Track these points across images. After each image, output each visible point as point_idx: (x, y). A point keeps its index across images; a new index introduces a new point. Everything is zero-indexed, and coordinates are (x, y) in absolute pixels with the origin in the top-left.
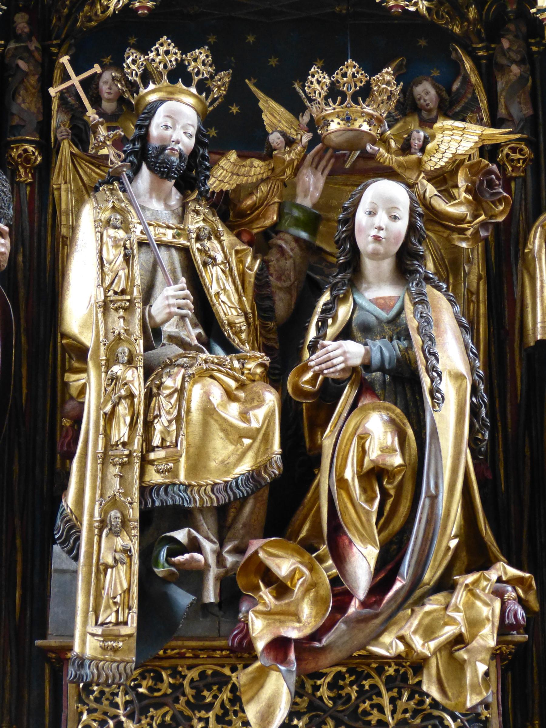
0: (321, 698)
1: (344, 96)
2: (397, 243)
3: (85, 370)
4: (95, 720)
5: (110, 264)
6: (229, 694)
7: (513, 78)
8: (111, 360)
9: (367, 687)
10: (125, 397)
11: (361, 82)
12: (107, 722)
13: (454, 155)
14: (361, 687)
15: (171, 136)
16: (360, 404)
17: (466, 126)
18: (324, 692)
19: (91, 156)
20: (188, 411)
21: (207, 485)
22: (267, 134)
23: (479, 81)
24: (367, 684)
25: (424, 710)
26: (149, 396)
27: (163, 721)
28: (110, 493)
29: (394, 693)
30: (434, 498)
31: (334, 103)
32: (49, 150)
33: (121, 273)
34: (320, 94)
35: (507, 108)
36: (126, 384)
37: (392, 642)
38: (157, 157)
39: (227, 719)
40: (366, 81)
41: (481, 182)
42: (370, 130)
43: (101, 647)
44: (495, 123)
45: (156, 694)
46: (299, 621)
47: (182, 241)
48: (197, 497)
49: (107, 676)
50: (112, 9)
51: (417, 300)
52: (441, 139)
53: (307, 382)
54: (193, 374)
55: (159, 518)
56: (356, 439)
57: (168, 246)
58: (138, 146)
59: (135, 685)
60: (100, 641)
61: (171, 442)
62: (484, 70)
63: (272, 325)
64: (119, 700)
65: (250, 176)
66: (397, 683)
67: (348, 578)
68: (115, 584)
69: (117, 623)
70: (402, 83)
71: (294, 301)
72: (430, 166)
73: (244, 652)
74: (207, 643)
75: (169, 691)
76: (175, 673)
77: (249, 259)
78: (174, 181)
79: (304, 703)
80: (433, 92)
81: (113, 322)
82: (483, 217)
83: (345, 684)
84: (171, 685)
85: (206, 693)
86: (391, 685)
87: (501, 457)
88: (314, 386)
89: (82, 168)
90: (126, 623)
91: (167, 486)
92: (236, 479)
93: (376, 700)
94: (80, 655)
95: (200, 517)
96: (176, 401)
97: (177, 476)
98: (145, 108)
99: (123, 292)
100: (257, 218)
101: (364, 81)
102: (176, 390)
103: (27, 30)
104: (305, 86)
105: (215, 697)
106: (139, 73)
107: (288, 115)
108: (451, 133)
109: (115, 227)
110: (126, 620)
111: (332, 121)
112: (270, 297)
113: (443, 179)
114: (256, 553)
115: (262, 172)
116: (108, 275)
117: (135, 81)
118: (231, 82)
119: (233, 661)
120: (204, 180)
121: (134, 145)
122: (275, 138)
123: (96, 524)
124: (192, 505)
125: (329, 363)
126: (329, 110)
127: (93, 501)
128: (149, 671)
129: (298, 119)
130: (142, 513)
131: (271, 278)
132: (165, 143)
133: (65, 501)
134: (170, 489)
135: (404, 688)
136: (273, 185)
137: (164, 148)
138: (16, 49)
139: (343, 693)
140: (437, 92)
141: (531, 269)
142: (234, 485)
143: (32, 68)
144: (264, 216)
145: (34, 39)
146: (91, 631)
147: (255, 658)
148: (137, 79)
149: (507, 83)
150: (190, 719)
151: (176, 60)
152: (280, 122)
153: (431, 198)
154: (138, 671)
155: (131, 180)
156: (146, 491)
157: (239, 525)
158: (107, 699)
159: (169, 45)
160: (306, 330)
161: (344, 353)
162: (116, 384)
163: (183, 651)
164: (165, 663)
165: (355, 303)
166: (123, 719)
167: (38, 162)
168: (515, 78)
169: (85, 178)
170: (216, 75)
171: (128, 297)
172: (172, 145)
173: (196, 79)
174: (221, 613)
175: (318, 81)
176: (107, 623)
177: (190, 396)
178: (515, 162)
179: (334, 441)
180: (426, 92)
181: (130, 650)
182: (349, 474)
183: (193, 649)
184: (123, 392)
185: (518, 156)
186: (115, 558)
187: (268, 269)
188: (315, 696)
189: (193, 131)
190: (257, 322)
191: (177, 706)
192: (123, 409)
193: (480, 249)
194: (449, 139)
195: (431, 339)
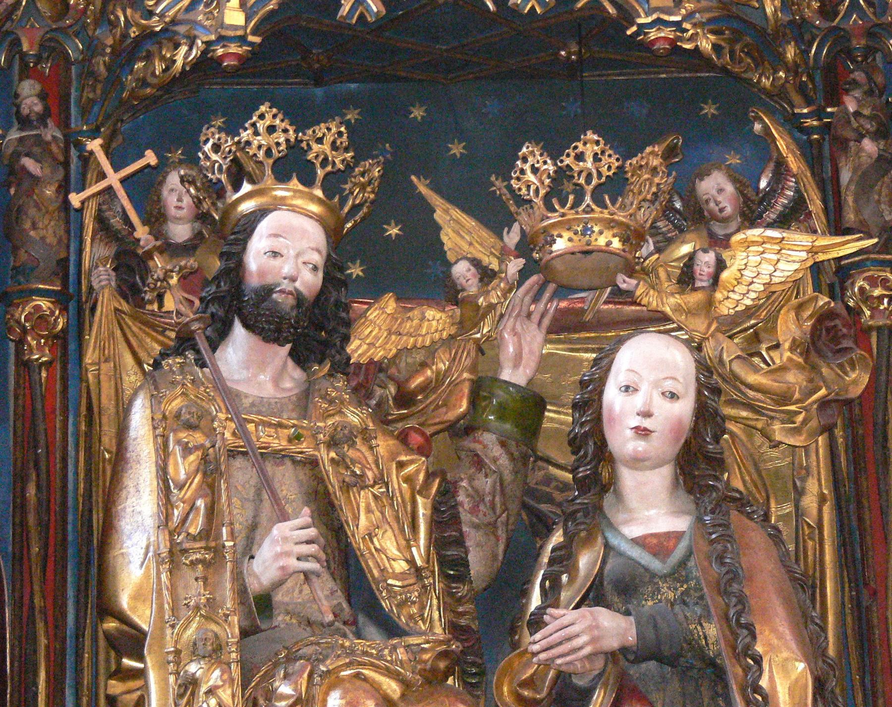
2: (677, 439)
3: (140, 674)
5: (181, 489)
7: (864, 159)
13: (768, 285)
17: (785, 235)
22: (449, 265)
31: (563, 205)
32: (75, 301)
33: (200, 503)
34: (537, 191)
35: (858, 211)
38: (257, 305)
42: (624, 250)
44: (837, 227)
47: (305, 447)
50: (179, 62)
51: (714, 536)
52: (745, 261)
57: (280, 456)
63: (462, 590)
65: (420, 335)
70: (674, 173)
78: (288, 346)
80: (730, 188)
81: (186, 587)
82: (823, 392)
89: (134, 335)
98: (236, 225)
103: (39, 108)
104: (512, 178)
106: (224, 167)
107: (485, 233)
108: (761, 249)
109: (191, 427)
111: (560, 236)
112: (460, 542)
113: (752, 329)
115: (440, 329)
116: (177, 507)
117: (219, 181)
118: (381, 177)
121: (218, 286)
122: (461, 270)
126: (554, 218)
129: (502, 239)
131: (461, 509)
136: (460, 351)
138: (21, 139)
143: (47, 171)
145: (50, 123)
148: (223, 178)
149: (855, 170)
151: (287, 141)
152: (471, 244)
153: (731, 362)
155: (214, 347)
159: (274, 116)
160: (525, 594)
161: (591, 628)
167: (60, 327)
168: (869, 160)
170: (356, 164)
171: (213, 544)
172: (286, 285)
175: (533, 169)
189: (317, 259)
193: (821, 451)
194: (758, 259)
195: (742, 600)
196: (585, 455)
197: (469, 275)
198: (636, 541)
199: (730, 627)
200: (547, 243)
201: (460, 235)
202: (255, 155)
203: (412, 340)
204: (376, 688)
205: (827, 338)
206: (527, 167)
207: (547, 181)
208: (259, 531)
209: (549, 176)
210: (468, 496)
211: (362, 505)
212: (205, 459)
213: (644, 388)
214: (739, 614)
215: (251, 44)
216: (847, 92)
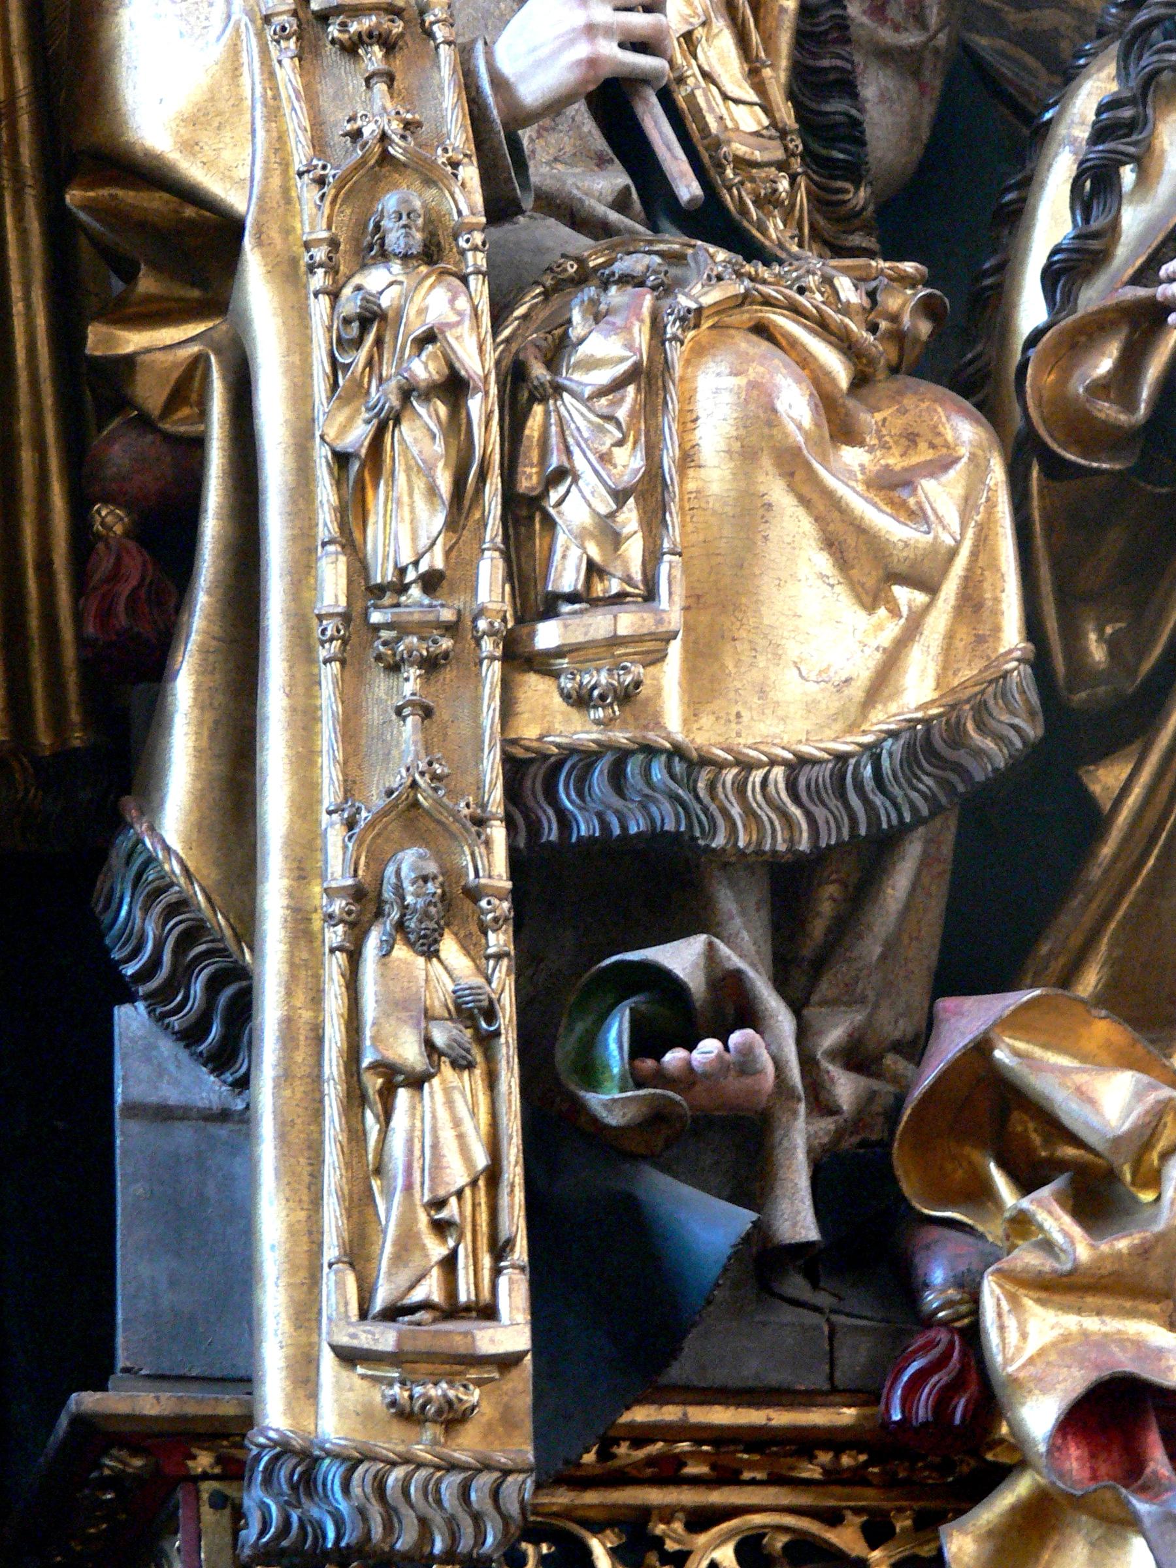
10: (429, 393)
20: (688, 459)
21: (773, 763)
48: (736, 811)
49: (424, 1523)
53: (1100, 388)
54: (699, 310)
63: (860, 196)
69: (452, 1310)
71: (929, 109)
74: (781, 1418)
88: (1129, 405)
90: (488, 1312)
91: (622, 756)
92: (873, 751)
94: (297, 1443)
96: (633, 414)
102: (633, 375)
112: (847, 86)
114: (982, 1048)
119: (870, 1497)
123: (338, 906)
124: (719, 841)
133: (152, 829)
134: (632, 767)
146: (344, 1340)
147: (993, 1478)
162: (379, 342)
163: (685, 1446)
177: (688, 399)
181: (507, 1419)
183: (723, 1438)
186: (429, 1045)
192: (420, 437)
204: (805, 361)
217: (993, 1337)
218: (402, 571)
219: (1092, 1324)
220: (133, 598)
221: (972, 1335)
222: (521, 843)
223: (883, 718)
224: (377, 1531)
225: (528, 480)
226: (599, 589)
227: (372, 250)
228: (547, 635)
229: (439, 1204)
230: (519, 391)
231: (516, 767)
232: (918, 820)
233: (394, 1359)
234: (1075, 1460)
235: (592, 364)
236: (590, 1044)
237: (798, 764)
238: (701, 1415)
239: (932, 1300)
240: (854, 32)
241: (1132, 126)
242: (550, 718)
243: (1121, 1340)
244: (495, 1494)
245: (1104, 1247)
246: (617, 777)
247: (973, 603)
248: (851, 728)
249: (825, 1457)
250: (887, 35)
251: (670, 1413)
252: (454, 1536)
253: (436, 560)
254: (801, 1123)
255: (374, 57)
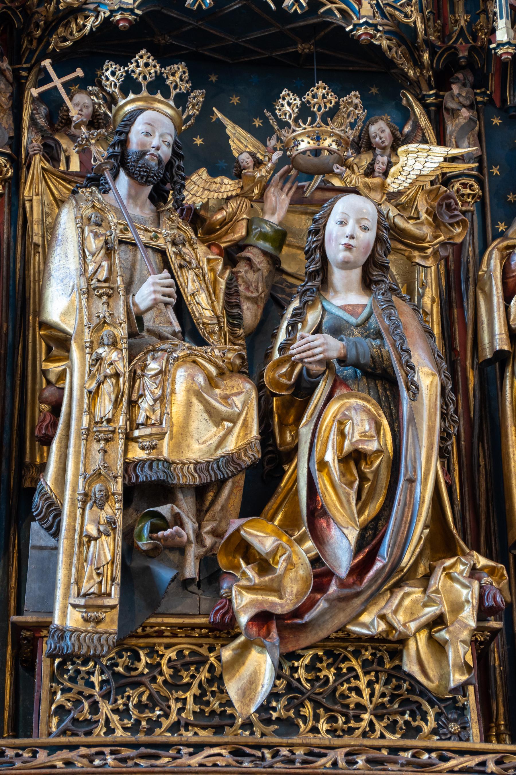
0: (299, 680)
1: (313, 115)
2: (366, 253)
4: (69, 700)
6: (207, 675)
8: (95, 343)
9: (344, 670)
10: (111, 376)
11: (331, 103)
12: (81, 702)
14: (339, 669)
15: (151, 143)
16: (336, 396)
18: (302, 674)
19: (62, 172)
20: (173, 392)
21: (190, 463)
23: (429, 125)
24: (344, 666)
25: (402, 695)
26: (133, 377)
27: (140, 701)
28: (93, 467)
29: (372, 676)
30: (411, 481)
31: (305, 123)
34: (290, 116)
36: (111, 364)
37: (374, 620)
39: (204, 699)
40: (336, 102)
41: (440, 205)
43: (83, 617)
45: (133, 673)
46: (281, 598)
47: (161, 243)
48: (180, 475)
49: (88, 647)
50: (88, 28)
54: (178, 357)
55: (146, 492)
56: (336, 423)
58: (117, 149)
59: (111, 664)
60: (82, 612)
61: (156, 420)
62: (432, 116)
63: (240, 332)
64: (96, 679)
66: (375, 666)
67: (328, 558)
68: (99, 555)
69: (100, 595)
71: (260, 311)
72: (393, 188)
73: (224, 629)
74: (187, 621)
75: (146, 671)
76: (152, 652)
77: (220, 267)
79: (282, 684)
80: (388, 131)
82: (442, 238)
83: (323, 666)
84: (147, 665)
85: (184, 673)
86: (369, 669)
87: (456, 467)
88: (290, 379)
90: (109, 595)
91: (152, 461)
92: (217, 460)
93: (354, 683)
94: (61, 628)
95: (180, 496)
96: (160, 382)
97: (161, 453)
99: (106, 281)
100: (226, 233)
101: (333, 102)
102: (161, 372)
105: (193, 677)
108: (416, 155)
110: (108, 591)
111: (303, 141)
112: (238, 306)
114: (238, 530)
118: (203, 102)
119: (211, 641)
120: (180, 189)
122: (245, 159)
123: (80, 498)
124: (175, 482)
125: (310, 353)
126: (300, 131)
127: (76, 475)
128: (127, 650)
130: (125, 488)
132: (145, 149)
134: (154, 464)
135: (381, 672)
137: (144, 153)
139: (321, 675)
140: (391, 131)
141: (487, 289)
142: (215, 466)
144: (233, 230)
146: (72, 602)
147: (237, 635)
148: (117, 90)
149: (457, 125)
150: (167, 699)
151: (156, 72)
154: (115, 650)
156: (129, 466)
157: (217, 507)
158: (83, 678)
159: (149, 58)
160: (275, 336)
161: (323, 344)
162: (100, 365)
163: (164, 628)
164: (142, 642)
165: (324, 309)
166: (98, 698)
169: (56, 192)
172: (153, 151)
173: (174, 93)
174: (200, 592)
176: (90, 594)
178: (466, 197)
179: (312, 427)
180: (380, 130)
181: (112, 621)
182: (330, 456)
183: (172, 626)
184: (109, 371)
185: (468, 191)
186: (99, 530)
187: (237, 280)
188: (293, 677)
189: (170, 139)
190: (226, 329)
191: (154, 686)
192: (107, 387)
196: (314, 259)
197: (248, 161)
198: (340, 307)
199: (397, 351)
200: (295, 145)
201: (240, 142)
202: (137, 78)
203: (216, 194)
204: (204, 369)
205: (443, 210)
206: (285, 103)
207: (296, 110)
208: (134, 286)
209: (297, 107)
210: (244, 282)
211: (190, 278)
212: (106, 242)
213: (351, 222)
214: (402, 344)
215: (136, 15)
216: (454, 83)
217: (234, 601)
218: (102, 418)
219: (260, 597)
220: (47, 427)
221: (230, 600)
222: (127, 482)
223: (220, 452)
224: (76, 649)
225: (134, 397)
226: (149, 422)
227: (102, 344)
228: (136, 433)
229: (98, 569)
230: (133, 377)
231: (126, 465)
232: (230, 477)
233: (85, 606)
234: (254, 631)
235: (152, 370)
236: (141, 530)
237: (197, 463)
238: (167, 620)
239: (223, 591)
240: (241, 294)
241: (301, 314)
242: (137, 453)
243: (266, 601)
244: (107, 639)
245: (262, 579)
246: (150, 467)
247: (245, 425)
248: (212, 455)
249: (198, 630)
250: (249, 294)
251: (159, 620)
252: (96, 650)
253: (110, 416)
254: (193, 549)
255: (105, 298)
